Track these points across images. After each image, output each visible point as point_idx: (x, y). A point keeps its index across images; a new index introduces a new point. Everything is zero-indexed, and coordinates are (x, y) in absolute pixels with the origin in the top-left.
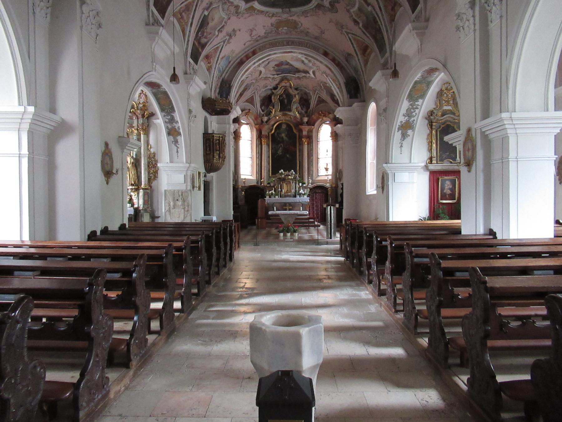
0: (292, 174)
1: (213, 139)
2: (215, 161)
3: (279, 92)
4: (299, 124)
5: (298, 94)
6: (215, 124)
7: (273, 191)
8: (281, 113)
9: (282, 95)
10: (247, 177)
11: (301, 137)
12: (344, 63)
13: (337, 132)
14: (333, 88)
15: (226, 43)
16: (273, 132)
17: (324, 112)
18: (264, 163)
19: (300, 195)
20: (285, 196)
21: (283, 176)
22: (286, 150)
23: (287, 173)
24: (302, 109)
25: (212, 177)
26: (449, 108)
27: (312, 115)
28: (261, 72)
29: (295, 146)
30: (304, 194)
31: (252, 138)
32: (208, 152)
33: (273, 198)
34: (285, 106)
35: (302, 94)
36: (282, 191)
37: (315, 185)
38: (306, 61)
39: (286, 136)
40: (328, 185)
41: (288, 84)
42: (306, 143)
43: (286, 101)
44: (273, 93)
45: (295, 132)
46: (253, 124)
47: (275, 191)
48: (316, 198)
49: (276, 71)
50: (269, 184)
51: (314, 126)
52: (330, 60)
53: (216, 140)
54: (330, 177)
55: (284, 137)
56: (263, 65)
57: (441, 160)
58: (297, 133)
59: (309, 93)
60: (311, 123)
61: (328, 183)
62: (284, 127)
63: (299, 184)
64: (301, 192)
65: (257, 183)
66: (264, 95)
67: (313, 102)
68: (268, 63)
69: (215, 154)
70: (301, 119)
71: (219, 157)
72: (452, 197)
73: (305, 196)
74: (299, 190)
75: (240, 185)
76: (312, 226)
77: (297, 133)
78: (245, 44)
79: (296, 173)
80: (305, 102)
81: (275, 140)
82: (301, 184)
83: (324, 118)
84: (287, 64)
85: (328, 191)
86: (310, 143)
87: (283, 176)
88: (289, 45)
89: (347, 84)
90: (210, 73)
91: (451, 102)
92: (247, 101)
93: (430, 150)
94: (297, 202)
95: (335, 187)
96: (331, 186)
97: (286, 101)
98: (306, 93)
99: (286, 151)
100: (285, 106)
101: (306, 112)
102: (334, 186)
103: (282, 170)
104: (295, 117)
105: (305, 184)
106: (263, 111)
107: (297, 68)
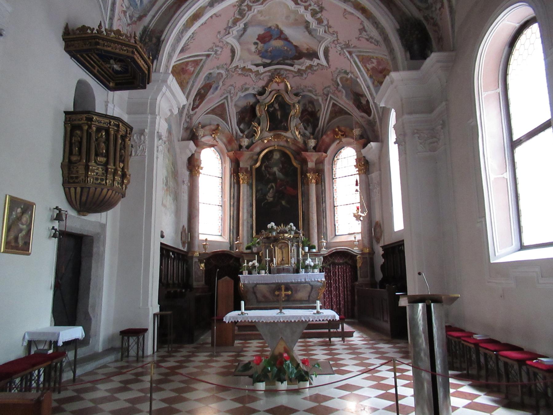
0: (291, 230)
1: (90, 127)
2: (91, 180)
3: (268, 100)
4: (300, 151)
5: (299, 102)
6: (112, 103)
8: (271, 134)
9: (272, 104)
10: (210, 238)
11: (304, 173)
13: (369, 157)
14: (361, 81)
16: (258, 164)
17: (343, 128)
18: (244, 215)
19: (306, 267)
20: (279, 271)
21: (274, 234)
22: (279, 193)
24: (306, 129)
25: (103, 227)
27: (322, 136)
28: (233, 51)
29: (296, 188)
30: (314, 267)
31: (223, 173)
32: (74, 158)
33: (255, 275)
34: (278, 122)
35: (305, 105)
36: (272, 261)
37: (333, 249)
38: (314, 24)
39: (281, 170)
40: (356, 250)
42: (313, 181)
43: (279, 113)
44: (258, 102)
45: (295, 164)
46: (225, 151)
47: (259, 261)
48: (335, 275)
49: (262, 54)
50: (248, 248)
51: (326, 152)
53: (99, 130)
54: (359, 237)
55: (277, 172)
56: (235, 31)
59: (318, 100)
60: (321, 148)
61: (355, 246)
62: (276, 156)
63: (303, 249)
64: (307, 262)
65: (231, 248)
66: (243, 103)
67: (324, 116)
68: (245, 29)
69: (92, 163)
73: (316, 271)
74: (304, 260)
76: (337, 335)
79: (297, 227)
80: (310, 117)
81: (261, 177)
82: (307, 249)
83: (344, 140)
84: (279, 38)
86: (320, 181)
87: (274, 234)
89: (402, 33)
92: (213, 111)
94: (301, 283)
95: (369, 253)
96: (362, 251)
97: (279, 113)
99: (280, 194)
100: (278, 122)
101: (313, 134)
102: (367, 251)
103: (273, 224)
104: (295, 140)
105: (314, 247)
106: (242, 131)
107: (296, 47)
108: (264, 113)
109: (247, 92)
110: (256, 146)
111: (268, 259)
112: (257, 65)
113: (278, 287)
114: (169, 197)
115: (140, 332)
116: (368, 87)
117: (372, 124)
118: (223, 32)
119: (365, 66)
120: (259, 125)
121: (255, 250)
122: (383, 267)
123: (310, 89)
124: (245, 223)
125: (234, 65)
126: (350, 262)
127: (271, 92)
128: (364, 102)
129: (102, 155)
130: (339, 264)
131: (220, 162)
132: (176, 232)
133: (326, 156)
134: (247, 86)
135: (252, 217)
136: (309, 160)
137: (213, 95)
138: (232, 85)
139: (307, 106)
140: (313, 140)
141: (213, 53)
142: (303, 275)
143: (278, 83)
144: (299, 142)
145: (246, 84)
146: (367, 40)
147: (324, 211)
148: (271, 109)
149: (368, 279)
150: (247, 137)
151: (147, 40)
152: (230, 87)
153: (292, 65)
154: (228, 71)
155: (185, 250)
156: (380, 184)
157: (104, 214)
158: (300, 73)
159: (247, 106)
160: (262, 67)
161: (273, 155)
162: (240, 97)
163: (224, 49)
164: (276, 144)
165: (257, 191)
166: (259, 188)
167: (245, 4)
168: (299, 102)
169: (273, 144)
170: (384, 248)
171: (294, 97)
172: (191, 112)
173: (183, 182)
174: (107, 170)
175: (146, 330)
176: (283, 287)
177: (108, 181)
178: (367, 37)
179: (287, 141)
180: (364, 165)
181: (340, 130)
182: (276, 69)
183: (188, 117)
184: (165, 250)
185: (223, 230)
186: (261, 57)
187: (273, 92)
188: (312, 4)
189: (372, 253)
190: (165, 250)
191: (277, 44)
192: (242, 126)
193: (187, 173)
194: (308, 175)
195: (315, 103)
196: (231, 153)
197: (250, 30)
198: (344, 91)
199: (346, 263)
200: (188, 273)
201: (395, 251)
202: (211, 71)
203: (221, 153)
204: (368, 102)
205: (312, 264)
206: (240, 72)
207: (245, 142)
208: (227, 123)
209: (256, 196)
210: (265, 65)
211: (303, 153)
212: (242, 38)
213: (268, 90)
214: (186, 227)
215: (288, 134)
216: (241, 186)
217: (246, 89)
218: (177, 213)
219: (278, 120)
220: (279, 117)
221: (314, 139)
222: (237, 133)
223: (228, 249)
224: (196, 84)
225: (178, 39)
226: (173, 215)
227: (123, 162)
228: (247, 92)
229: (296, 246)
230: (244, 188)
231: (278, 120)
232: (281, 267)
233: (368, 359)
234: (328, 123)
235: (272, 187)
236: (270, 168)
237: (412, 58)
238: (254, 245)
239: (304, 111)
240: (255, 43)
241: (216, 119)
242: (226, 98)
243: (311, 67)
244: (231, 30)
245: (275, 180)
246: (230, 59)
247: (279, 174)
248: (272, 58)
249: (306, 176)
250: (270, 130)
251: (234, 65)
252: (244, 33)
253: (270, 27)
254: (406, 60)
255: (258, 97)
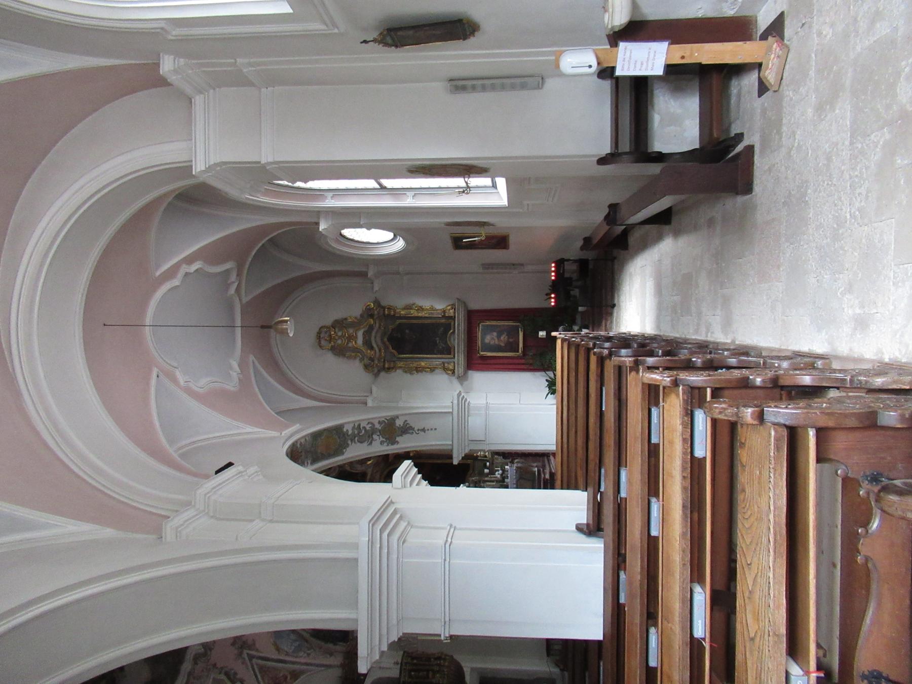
15: (253, 653)
25: (473, 669)
26: (360, 334)
53: (410, 676)
57: (448, 351)
71: (438, 672)
72: (513, 332)
82: (486, 471)
90: (302, 672)
91: (351, 331)
93: (432, 370)
157: (465, 669)
174: (438, 672)
205: (500, 472)
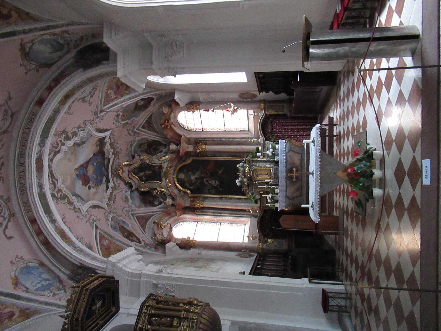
0: (242, 166)
3: (136, 181)
4: (179, 157)
5: (140, 156)
7: (268, 196)
8: (164, 179)
10: (247, 234)
11: (197, 154)
12: (54, 72)
13: (187, 101)
14: (125, 104)
16: (188, 192)
17: (162, 121)
18: (229, 205)
19: (274, 155)
20: (276, 177)
21: (245, 180)
22: (212, 175)
23: (240, 174)
24: (161, 151)
25: (233, 323)
27: (167, 138)
28: (95, 207)
29: (209, 161)
30: (274, 148)
33: (279, 197)
35: (142, 151)
36: (267, 183)
37: (260, 133)
38: (76, 139)
39: (194, 173)
40: (261, 114)
41: (126, 169)
42: (204, 147)
43: (148, 172)
44: (137, 189)
45: (189, 161)
46: (175, 218)
47: (268, 193)
48: (281, 132)
49: (98, 183)
50: (256, 202)
51: (181, 136)
52: (49, 95)
53: (150, 322)
54: (251, 112)
55: (196, 176)
58: (191, 159)
60: (177, 139)
61: (258, 114)
63: (259, 157)
65: (255, 216)
66: (138, 201)
67: (152, 136)
68: (77, 196)
70: (173, 152)
73: (277, 147)
74: (268, 156)
75: (257, 244)
77: (191, 159)
78: (10, 238)
80: (152, 147)
81: (199, 190)
82: (259, 154)
83: (172, 121)
84: (86, 168)
85: (271, 115)
86: (205, 141)
88: (24, 163)
89: (87, 66)
90: (36, 312)
92: (143, 226)
94: (286, 159)
95: (264, 104)
96: (262, 109)
97: (148, 172)
98: (140, 145)
99: (213, 175)
101: (165, 146)
102: (262, 105)
103: (237, 181)
104: (170, 160)
105: (258, 149)
106: (160, 203)
108: (146, 185)
109: (129, 197)
110: (173, 192)
111: (266, 186)
112: (107, 188)
113: (289, 178)
114: (211, 266)
115: (325, 297)
116: (130, 98)
117: (160, 97)
118: (78, 214)
119: (113, 100)
120: (156, 189)
121: (258, 197)
122: (276, 93)
123: (129, 147)
124: (236, 204)
125: (106, 207)
126: (271, 119)
127: (130, 178)
128: (142, 103)
129: (172, 322)
130: (272, 129)
131: (184, 222)
132: (241, 261)
133: (184, 135)
134: (124, 197)
135: (230, 198)
136: (187, 150)
137: (130, 225)
138: (123, 210)
139: (143, 149)
140: (171, 146)
141: (95, 223)
142: (281, 158)
143: (123, 172)
144: (172, 157)
145: (122, 198)
146: (92, 96)
147: (228, 139)
148: (144, 178)
149: (285, 105)
150: (166, 200)
151: (80, 277)
152: (124, 211)
153: (109, 160)
154: (110, 212)
155: (256, 255)
156: (208, 93)
157: (222, 322)
158: (116, 153)
159: (140, 198)
160: (109, 184)
161: (181, 179)
162: (132, 203)
163: (92, 213)
164: (172, 176)
165: (210, 193)
166: (207, 191)
167: (56, 194)
168: (140, 156)
169: (172, 179)
170: (260, 91)
171: (135, 160)
172: (143, 244)
173: (199, 253)
174: (185, 318)
175: (323, 290)
176: (289, 174)
177: (194, 318)
178: (89, 97)
179: (170, 167)
180: (193, 105)
181: (164, 124)
182: (112, 173)
183: (146, 247)
184: (255, 272)
185: (241, 223)
186: (100, 185)
187: (130, 176)
188: (60, 139)
189: (264, 101)
190: (255, 272)
191: (90, 171)
192: (156, 203)
193: (192, 250)
194: (198, 151)
195: (141, 142)
196: (178, 213)
197: (78, 192)
198: (133, 119)
199: (271, 123)
200: (276, 253)
201: (264, 80)
202: (110, 226)
203: (177, 222)
204: (142, 100)
205: (271, 150)
206: (112, 202)
207: (169, 201)
208: (153, 215)
209: (214, 194)
210: (108, 181)
211: (180, 154)
212: (84, 198)
213: (128, 180)
214: (236, 253)
215: (165, 166)
216: (205, 206)
217: (126, 197)
218: (225, 260)
219: (152, 173)
220: (151, 172)
221: (170, 145)
222: (161, 208)
223: (256, 219)
224: (120, 239)
225: (81, 251)
226: (227, 264)
227: (179, 303)
228: (129, 197)
229: (256, 163)
230: (207, 204)
231: (152, 173)
232: (273, 175)
233: (353, 103)
234: (157, 133)
235: (207, 181)
236: (191, 182)
237: (107, 59)
238: (254, 198)
239: (147, 152)
240: (89, 188)
241: (149, 224)
242: (132, 215)
243: (111, 144)
244: (77, 207)
245: (201, 178)
246: (100, 209)
247: (197, 175)
248: (102, 176)
249: (200, 152)
250: (160, 180)
251: (106, 207)
252: (80, 197)
253: (77, 175)
254: (108, 64)
255: (133, 188)
